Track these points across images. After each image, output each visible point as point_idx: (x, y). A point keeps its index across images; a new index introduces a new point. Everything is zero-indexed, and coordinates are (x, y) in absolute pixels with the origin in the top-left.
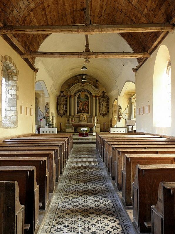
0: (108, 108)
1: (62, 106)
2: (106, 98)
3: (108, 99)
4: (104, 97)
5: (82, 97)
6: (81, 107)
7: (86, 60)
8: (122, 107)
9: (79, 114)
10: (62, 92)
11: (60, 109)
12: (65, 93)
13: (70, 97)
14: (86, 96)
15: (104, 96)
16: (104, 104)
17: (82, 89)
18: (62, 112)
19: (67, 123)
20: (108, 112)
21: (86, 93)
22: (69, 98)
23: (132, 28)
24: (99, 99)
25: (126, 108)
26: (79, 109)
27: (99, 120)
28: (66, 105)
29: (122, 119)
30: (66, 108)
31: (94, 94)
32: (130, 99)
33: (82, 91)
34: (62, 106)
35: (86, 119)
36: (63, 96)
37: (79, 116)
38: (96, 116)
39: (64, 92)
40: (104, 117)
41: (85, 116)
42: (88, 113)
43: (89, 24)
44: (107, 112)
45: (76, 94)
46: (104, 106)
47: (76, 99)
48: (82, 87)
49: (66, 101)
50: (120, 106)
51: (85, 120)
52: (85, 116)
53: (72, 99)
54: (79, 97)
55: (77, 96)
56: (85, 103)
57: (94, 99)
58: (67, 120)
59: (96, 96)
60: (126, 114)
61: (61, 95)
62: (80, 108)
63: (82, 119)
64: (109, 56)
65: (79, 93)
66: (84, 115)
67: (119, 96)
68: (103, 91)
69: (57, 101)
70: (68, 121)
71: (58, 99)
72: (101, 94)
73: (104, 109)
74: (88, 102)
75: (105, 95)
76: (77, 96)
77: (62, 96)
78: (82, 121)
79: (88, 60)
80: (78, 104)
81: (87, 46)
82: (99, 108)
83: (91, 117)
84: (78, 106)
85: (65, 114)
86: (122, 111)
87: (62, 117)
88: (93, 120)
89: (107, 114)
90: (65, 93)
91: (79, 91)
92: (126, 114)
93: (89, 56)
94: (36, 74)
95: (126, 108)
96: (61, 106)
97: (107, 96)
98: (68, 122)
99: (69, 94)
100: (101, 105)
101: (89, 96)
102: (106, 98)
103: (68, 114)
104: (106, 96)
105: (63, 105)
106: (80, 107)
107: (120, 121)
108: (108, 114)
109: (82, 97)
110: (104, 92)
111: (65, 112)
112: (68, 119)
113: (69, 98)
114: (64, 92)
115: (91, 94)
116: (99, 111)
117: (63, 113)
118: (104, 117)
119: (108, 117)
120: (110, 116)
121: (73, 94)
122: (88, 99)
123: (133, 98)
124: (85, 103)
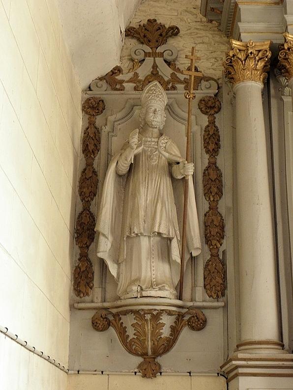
1: (154, 200)
11: (125, 236)
18: (151, 277)
22: (252, 88)
34: (154, 200)
36: (166, 72)
39: (174, 31)
61: (144, 71)
69: (91, 145)
71: (93, 107)
85: (198, 323)
111: (200, 297)
114: (174, 31)
117: (166, 296)
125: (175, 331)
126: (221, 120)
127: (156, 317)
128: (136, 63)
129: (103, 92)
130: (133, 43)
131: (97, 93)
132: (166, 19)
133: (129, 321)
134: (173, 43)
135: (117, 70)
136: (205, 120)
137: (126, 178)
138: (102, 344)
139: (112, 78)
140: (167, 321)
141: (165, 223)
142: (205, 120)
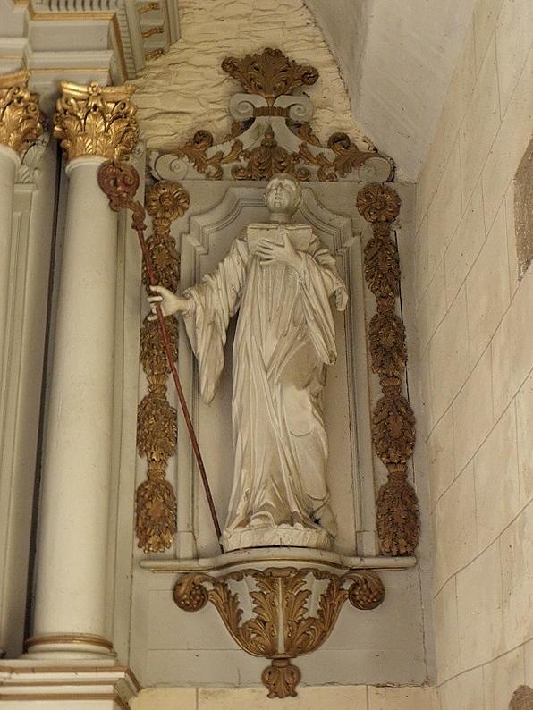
0: (396, 431)
2: (343, 191)
3: (384, 207)
16: (271, 289)
20: (401, 519)
40: (282, 679)
44: (356, 521)
46: (261, 343)
73: (275, 430)
75: (303, 129)
82: (157, 427)
89: (369, 594)
100: (206, 345)
102: (343, 191)
104: (340, 140)
108: (392, 581)
116: (153, 515)
118: (282, 679)
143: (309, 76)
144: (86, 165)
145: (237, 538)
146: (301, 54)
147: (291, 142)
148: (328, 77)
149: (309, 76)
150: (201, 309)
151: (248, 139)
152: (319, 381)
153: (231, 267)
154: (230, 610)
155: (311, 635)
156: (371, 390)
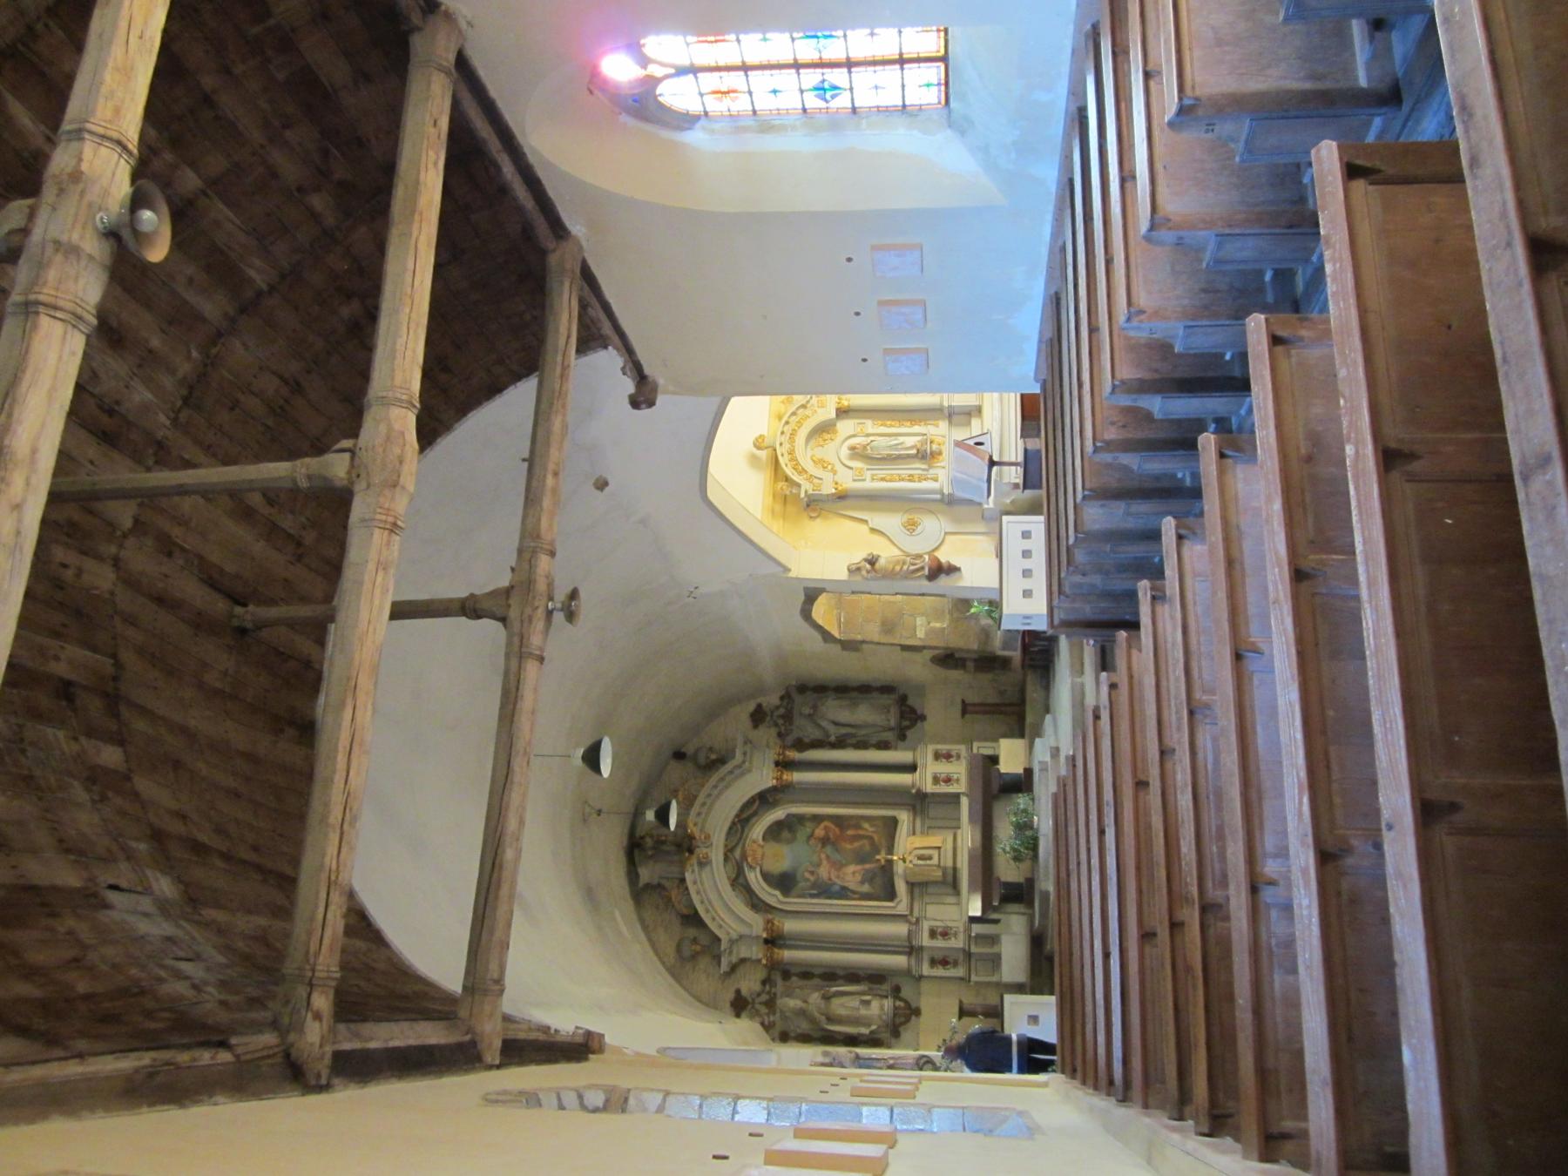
0: (865, 689)
1: (841, 1006)
2: (798, 699)
3: (802, 688)
4: (788, 717)
5: (781, 858)
6: (851, 868)
7: (559, 617)
8: (858, 556)
9: (901, 887)
10: (740, 1006)
11: (857, 1021)
12: (749, 983)
13: (774, 940)
14: (776, 831)
15: (782, 717)
16: (836, 712)
17: (726, 859)
18: (878, 1008)
19: (960, 972)
20: (887, 689)
21: (758, 830)
22: (787, 955)
23: (417, 217)
24: (800, 745)
25: (873, 530)
26: (866, 888)
27: (943, 748)
28: (831, 975)
29: (944, 556)
30: (852, 976)
31: (762, 777)
32: (815, 505)
33: (744, 857)
34: (841, 1006)
35: (934, 840)
36: (764, 997)
37: (912, 886)
38: (911, 768)
39: (738, 992)
40: (923, 718)
41: (919, 841)
42: (893, 823)
43: (352, 458)
44: (887, 700)
45: (756, 904)
46: (845, 716)
47: (794, 903)
48: (717, 855)
49: (806, 974)
50: (859, 569)
51: (944, 841)
52: (913, 845)
53: (790, 926)
54: (784, 882)
55: (771, 896)
56: (825, 841)
57: (797, 777)
58: (940, 971)
59: (777, 764)
60: (911, 526)
61: (764, 1010)
62: (859, 877)
63: (935, 861)
64: (551, 467)
65: (754, 878)
66: (909, 847)
67: (792, 574)
68: (747, 723)
70: (944, 963)
71: (784, 1037)
72: (766, 734)
73: (864, 714)
74: (817, 819)
75: (777, 708)
76: (771, 896)
77: (771, 1004)
78: (950, 863)
79: (560, 596)
80: (824, 890)
81: (470, 608)
82: (862, 745)
83: (919, 802)
84: (844, 893)
85: (896, 991)
86: (887, 554)
87: (917, 1012)
88: (943, 789)
90: (749, 983)
91: (739, 882)
92: (911, 526)
93: (541, 586)
94: (618, 1050)
95: (873, 530)
96: (842, 1012)
97: (786, 697)
98: (955, 964)
99: (756, 952)
100: (844, 731)
101: (778, 814)
102: (798, 699)
103: (900, 961)
104: (782, 698)
105: (836, 1002)
106: (852, 875)
107: (952, 570)
109: (781, 858)
110: (758, 717)
111: (886, 987)
112: (933, 963)
113: (787, 955)
114: (738, 992)
115: (765, 799)
117: (888, 1004)
118: (923, 718)
119: (921, 689)
120: (918, 670)
121: (756, 924)
122: (801, 819)
123: (806, 487)
124: (825, 841)
125: (901, 999)
126: (794, 970)
127: (896, 1008)
128: (757, 1013)
129: (776, 1032)
130: (744, 1015)
131: (776, 1034)
132: (730, 996)
133: (898, 1021)
134: (744, 992)
135: (762, 1024)
136: (794, 979)
137: (830, 1020)
138: (906, 1035)
139: (767, 1027)
140: (898, 1003)
141: (854, 1002)
142: (794, 979)
143: (759, 706)
144: (794, 755)
145: (893, 723)
146: (751, 707)
147: (782, 711)
148: (759, 700)
149: (759, 706)
150: (834, 733)
151: (781, 722)
152: (854, 705)
153: (824, 724)
154: (908, 728)
155: (913, 711)
156: (855, 694)
